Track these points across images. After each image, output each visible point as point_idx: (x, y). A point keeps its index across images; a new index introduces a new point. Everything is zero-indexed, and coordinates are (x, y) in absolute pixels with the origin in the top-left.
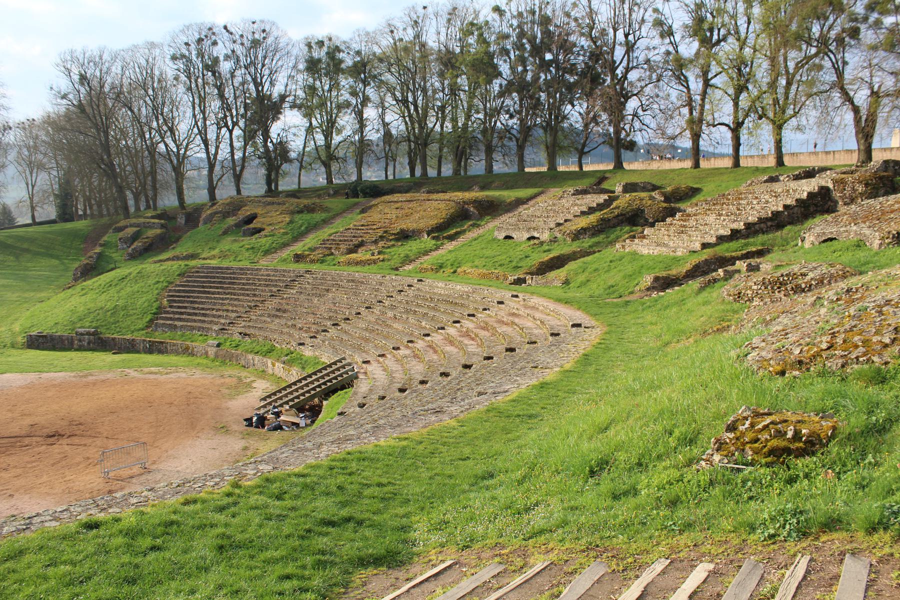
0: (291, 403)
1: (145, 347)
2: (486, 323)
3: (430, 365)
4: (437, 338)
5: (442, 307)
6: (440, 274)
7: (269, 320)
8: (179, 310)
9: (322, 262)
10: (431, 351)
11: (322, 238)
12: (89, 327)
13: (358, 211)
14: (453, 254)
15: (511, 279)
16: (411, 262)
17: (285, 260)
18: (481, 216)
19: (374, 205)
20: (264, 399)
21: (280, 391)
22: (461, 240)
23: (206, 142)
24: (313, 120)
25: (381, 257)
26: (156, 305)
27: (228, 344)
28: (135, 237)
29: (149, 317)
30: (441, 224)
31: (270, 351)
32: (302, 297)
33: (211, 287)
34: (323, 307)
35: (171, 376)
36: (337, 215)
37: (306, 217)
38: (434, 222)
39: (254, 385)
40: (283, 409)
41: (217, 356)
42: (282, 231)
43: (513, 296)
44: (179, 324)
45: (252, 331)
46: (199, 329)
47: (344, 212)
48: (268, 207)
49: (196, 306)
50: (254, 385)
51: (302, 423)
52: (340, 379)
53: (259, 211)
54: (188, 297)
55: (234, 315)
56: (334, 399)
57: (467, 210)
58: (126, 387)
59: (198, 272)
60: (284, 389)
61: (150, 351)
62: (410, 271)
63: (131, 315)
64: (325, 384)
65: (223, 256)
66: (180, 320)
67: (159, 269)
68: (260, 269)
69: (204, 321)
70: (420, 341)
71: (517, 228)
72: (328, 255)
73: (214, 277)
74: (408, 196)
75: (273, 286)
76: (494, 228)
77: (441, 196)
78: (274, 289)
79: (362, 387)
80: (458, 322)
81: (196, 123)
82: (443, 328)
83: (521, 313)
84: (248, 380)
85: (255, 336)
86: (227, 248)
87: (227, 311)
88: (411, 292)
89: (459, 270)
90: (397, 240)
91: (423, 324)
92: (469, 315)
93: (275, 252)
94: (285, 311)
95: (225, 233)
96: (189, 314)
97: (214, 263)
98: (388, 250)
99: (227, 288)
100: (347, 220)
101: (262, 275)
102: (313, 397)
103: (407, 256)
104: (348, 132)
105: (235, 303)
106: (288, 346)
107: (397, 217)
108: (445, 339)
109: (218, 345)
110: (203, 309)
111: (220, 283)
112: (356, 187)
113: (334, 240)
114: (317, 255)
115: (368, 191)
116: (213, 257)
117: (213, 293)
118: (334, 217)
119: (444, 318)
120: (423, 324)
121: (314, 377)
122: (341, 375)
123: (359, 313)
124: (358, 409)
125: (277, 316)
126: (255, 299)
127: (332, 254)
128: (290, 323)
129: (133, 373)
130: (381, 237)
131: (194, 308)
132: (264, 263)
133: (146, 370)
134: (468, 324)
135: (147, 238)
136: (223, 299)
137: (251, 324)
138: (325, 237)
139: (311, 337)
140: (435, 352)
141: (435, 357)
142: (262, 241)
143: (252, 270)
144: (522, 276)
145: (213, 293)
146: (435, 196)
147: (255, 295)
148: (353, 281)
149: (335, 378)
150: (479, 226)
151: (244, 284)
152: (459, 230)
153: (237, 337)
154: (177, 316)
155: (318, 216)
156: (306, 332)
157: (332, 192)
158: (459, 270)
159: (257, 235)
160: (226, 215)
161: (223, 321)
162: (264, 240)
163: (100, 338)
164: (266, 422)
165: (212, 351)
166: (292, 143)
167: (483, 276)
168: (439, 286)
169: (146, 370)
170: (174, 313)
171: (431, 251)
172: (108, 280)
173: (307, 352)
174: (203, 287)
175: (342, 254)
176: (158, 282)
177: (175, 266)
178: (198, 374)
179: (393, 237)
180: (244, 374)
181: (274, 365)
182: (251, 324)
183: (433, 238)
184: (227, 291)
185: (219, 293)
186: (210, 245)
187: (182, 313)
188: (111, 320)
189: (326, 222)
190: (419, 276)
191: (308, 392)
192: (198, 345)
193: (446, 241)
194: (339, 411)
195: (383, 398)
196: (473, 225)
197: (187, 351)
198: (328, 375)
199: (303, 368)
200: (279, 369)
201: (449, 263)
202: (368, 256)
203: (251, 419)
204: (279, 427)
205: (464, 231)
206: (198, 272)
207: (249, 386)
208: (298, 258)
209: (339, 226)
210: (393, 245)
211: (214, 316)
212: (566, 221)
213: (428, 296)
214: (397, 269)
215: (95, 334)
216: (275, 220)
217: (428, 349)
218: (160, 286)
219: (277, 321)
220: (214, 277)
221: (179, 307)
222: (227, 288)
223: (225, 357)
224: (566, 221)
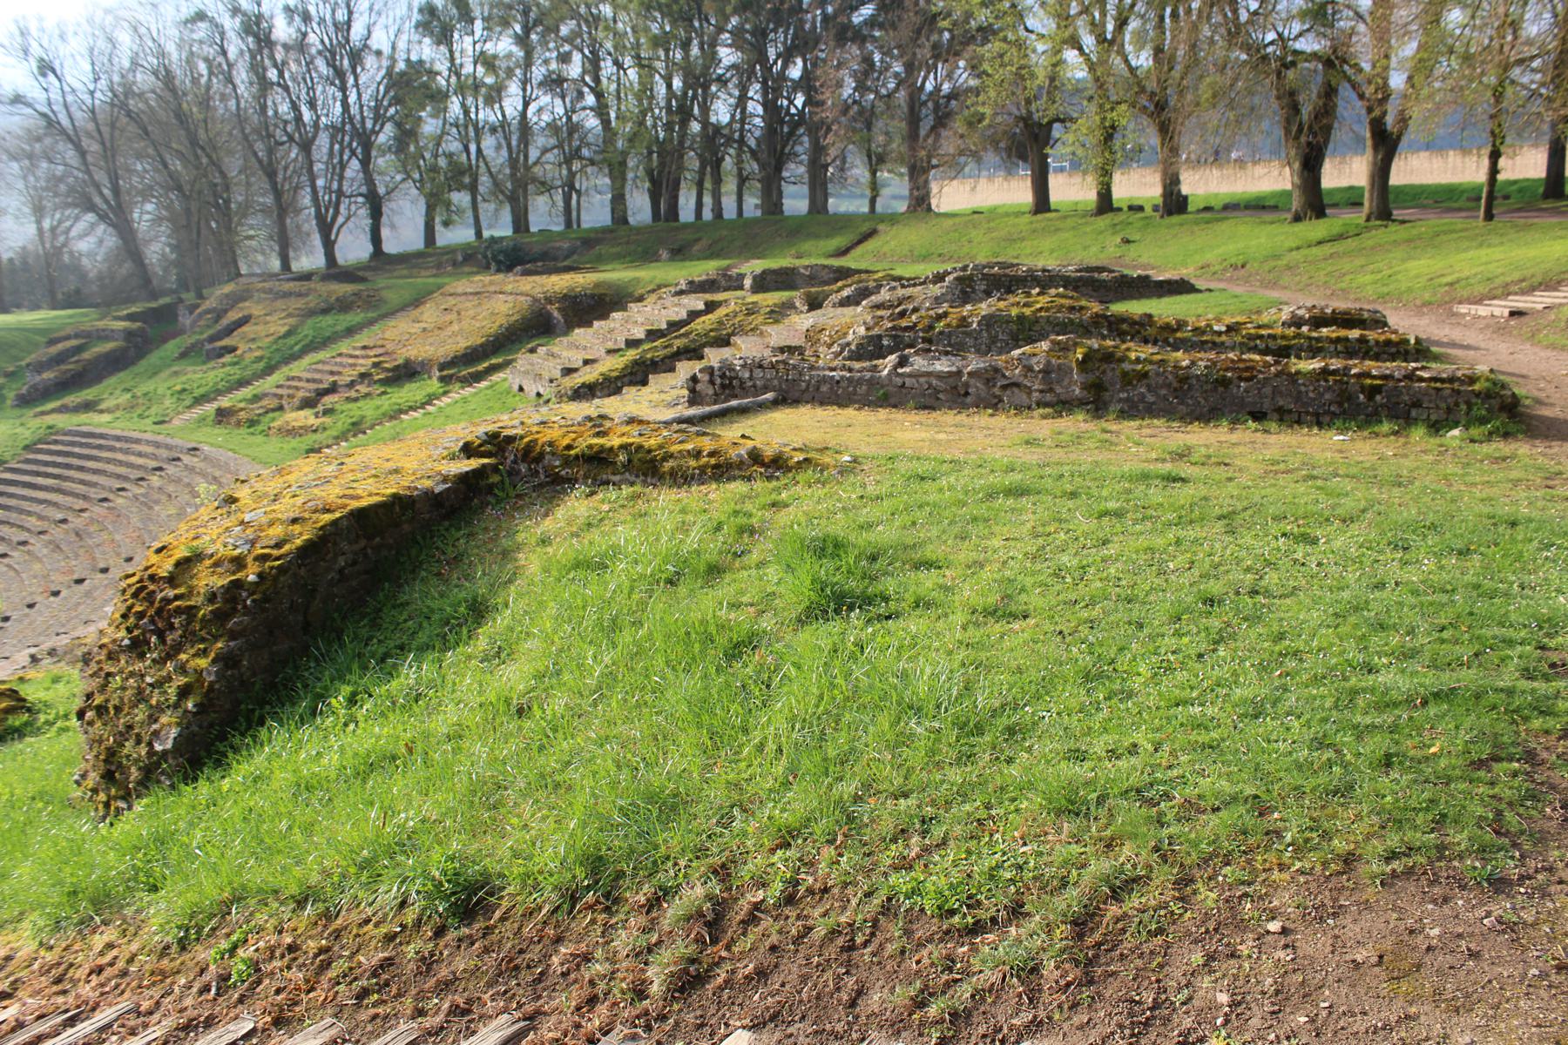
18: (569, 327)
28: (60, 359)
37: (327, 321)
38: (462, 344)
42: (258, 354)
53: (256, 310)
57: (549, 315)
59: (56, 442)
90: (387, 382)
114: (257, 409)
115: (501, 257)
127: (281, 408)
157: (460, 258)
159: (212, 364)
162: (212, 374)
174: (38, 474)
183: (442, 379)
189: (350, 332)
208: (222, 415)
210: (367, 395)
212: (586, 362)
224: (586, 362)
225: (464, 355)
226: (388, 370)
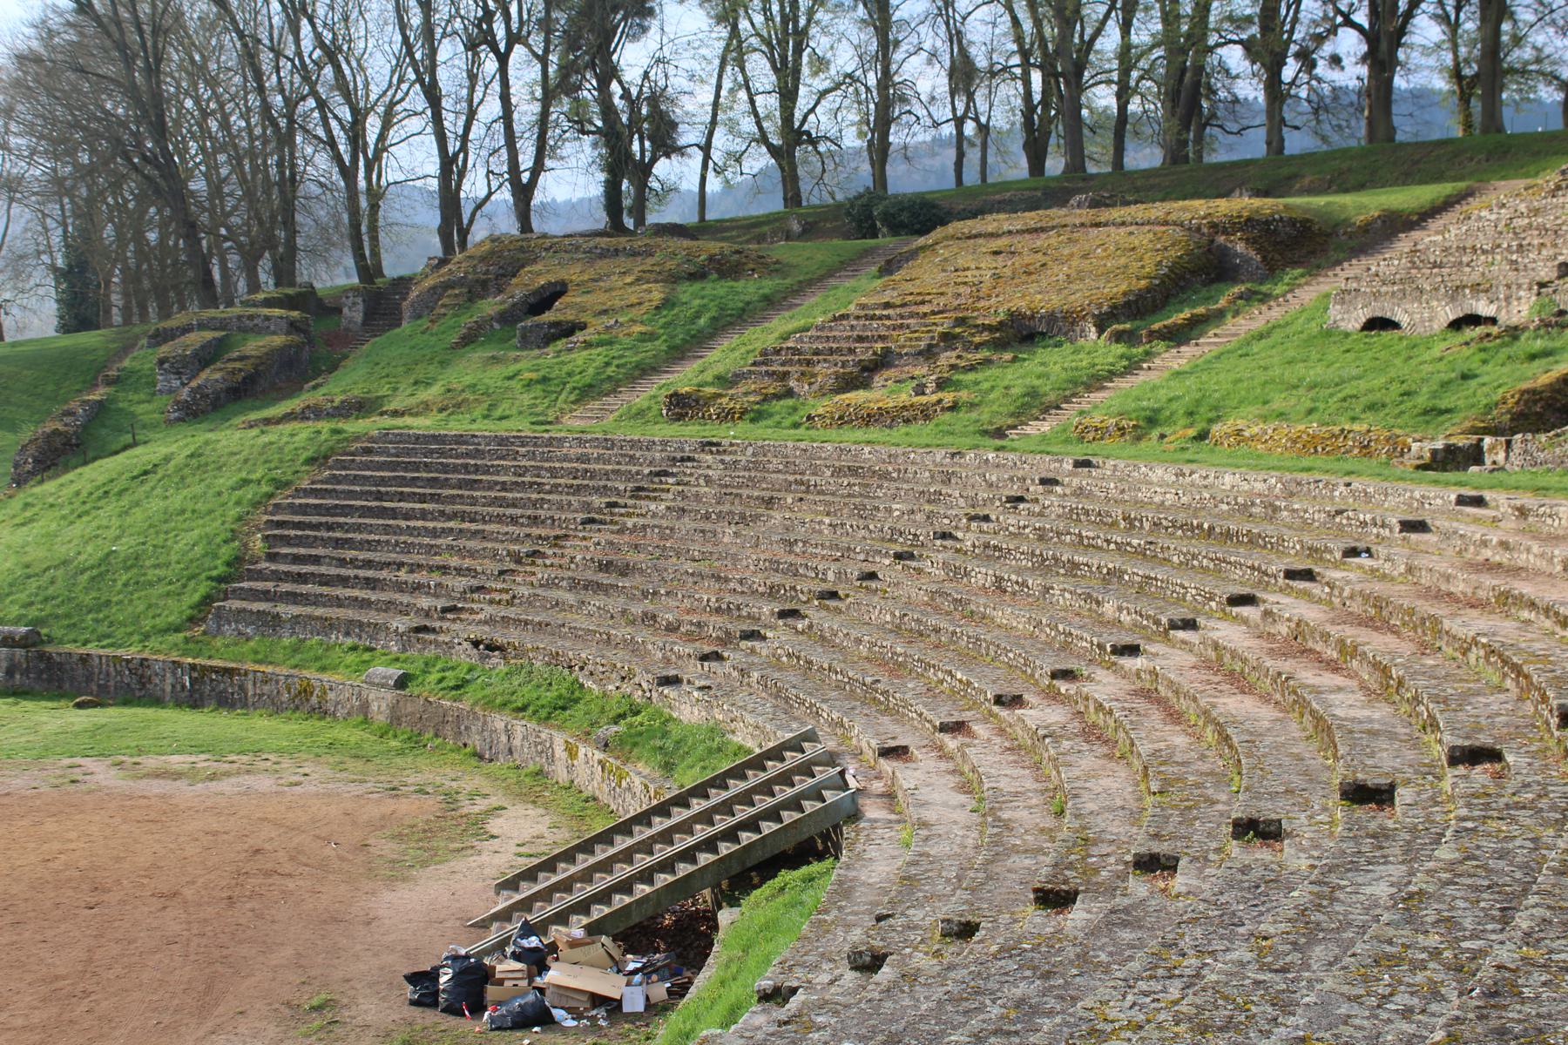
0: (599, 911)
1: (178, 686)
2: (1379, 603)
3: (1160, 777)
4: (1171, 660)
5: (1176, 546)
6: (1151, 443)
7: (570, 598)
8: (295, 568)
9: (758, 417)
10: (1156, 715)
11: (759, 346)
12: (17, 621)
13: (874, 269)
14: (1190, 382)
15: (1422, 448)
16: (1046, 410)
17: (641, 413)
18: (1272, 269)
19: (923, 248)
20: (511, 884)
21: (587, 847)
22: (1209, 343)
23: (433, 95)
24: (744, 24)
25: (948, 397)
26: (226, 552)
27: (434, 677)
28: (206, 357)
29: (204, 589)
30: (1140, 295)
31: (564, 705)
32: (687, 524)
33: (402, 497)
34: (748, 553)
35: (225, 786)
36: (810, 283)
37: (716, 289)
38: (1117, 289)
39: (494, 825)
40: (557, 933)
41: (395, 719)
42: (638, 328)
43: (1461, 501)
44: (287, 610)
45: (512, 636)
46: (349, 627)
47: (831, 273)
48: (602, 266)
49: (350, 554)
50: (494, 825)
51: (634, 1002)
52: (789, 816)
53: (572, 273)
54: (330, 527)
55: (461, 583)
56: (760, 904)
57: (1224, 252)
58: (50, 826)
59: (368, 451)
60: (606, 838)
61: (193, 700)
62: (1044, 438)
63: (151, 584)
64: (730, 835)
65: (453, 404)
66: (293, 598)
67: (256, 447)
68: (561, 440)
69: (365, 604)
70: (1100, 674)
71: (1408, 288)
72: (778, 397)
73: (416, 467)
74: (1031, 218)
75: (596, 490)
76: (1331, 299)
77: (1137, 211)
78: (598, 501)
79: (874, 859)
80: (1248, 600)
81: (410, 53)
82: (1190, 625)
83: (1522, 559)
84: (481, 805)
85: (520, 652)
86: (468, 380)
87: (444, 569)
88: (1053, 501)
89: (1216, 429)
90: (999, 345)
91: (1109, 609)
92: (1291, 575)
93: (614, 391)
94: (625, 570)
95: (468, 340)
96: (326, 581)
97: (422, 424)
98: (971, 376)
99: (452, 499)
100: (839, 293)
101: (566, 459)
102: (685, 887)
103: (1033, 393)
104: (844, 60)
105: (473, 544)
106: (627, 688)
107: (997, 277)
108: (1207, 665)
109: (402, 682)
110: (368, 564)
111: (433, 482)
112: (867, 208)
113: (795, 351)
114: (744, 395)
115: (904, 217)
116: (425, 408)
117: (407, 516)
118: (800, 289)
119: (1192, 585)
120: (1109, 609)
121: (698, 805)
122: (795, 804)
123: (872, 576)
124: (850, 977)
125: (598, 587)
126: (535, 531)
127: (790, 393)
128: (637, 609)
129: (102, 774)
130: (945, 337)
131: (342, 562)
132: (574, 422)
133: (151, 762)
134: (1291, 606)
135: (241, 359)
136: (434, 533)
137: (511, 612)
138: (771, 341)
139: (704, 658)
140: (1175, 717)
141: (1180, 741)
142: (579, 360)
143: (535, 442)
144: (1462, 441)
145: (407, 516)
146: (1116, 213)
147: (535, 520)
148: (853, 471)
149: (773, 814)
150: (1265, 298)
151: (504, 487)
152: (1200, 310)
153: (465, 656)
154: (286, 587)
155: (750, 288)
156: (690, 638)
157: (796, 227)
158: (1216, 429)
159: (561, 344)
160: (477, 289)
161: (424, 602)
162: (580, 357)
163: (42, 656)
164: (491, 991)
165: (381, 702)
166: (684, 99)
167: (1311, 445)
168: (1156, 479)
169: (151, 762)
170: (278, 577)
171: (1112, 375)
172: (101, 479)
173: (687, 710)
174: (379, 496)
175: (822, 393)
176: (246, 482)
177: (302, 436)
178: (317, 778)
179: (986, 336)
180: (471, 780)
181: (572, 752)
182: (511, 612)
183: (1118, 337)
184: (449, 509)
185: (424, 515)
186: (420, 372)
187: (301, 578)
188: (87, 600)
189: (772, 304)
190: (1079, 452)
191: (667, 866)
192: (339, 681)
193: (1160, 346)
194: (767, 984)
195: (966, 931)
196: (1248, 297)
197: (305, 702)
198: (746, 798)
199: (668, 767)
200: (585, 766)
201: (1179, 408)
202: (905, 396)
203: (433, 975)
204: (537, 1017)
205: (1220, 315)
206: (368, 451)
207: (477, 828)
208: (682, 406)
209: (813, 311)
211: (400, 587)
213: (1118, 512)
214: (1000, 433)
215: (26, 642)
216: (620, 299)
217: (1140, 704)
218: (249, 493)
219: (597, 601)
220: (416, 467)
221: (297, 559)
222: (452, 499)
223: (420, 726)
225: (1127, 304)
226: (989, 328)
